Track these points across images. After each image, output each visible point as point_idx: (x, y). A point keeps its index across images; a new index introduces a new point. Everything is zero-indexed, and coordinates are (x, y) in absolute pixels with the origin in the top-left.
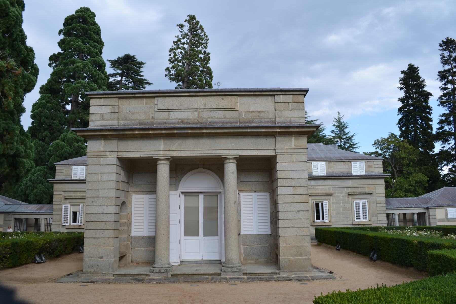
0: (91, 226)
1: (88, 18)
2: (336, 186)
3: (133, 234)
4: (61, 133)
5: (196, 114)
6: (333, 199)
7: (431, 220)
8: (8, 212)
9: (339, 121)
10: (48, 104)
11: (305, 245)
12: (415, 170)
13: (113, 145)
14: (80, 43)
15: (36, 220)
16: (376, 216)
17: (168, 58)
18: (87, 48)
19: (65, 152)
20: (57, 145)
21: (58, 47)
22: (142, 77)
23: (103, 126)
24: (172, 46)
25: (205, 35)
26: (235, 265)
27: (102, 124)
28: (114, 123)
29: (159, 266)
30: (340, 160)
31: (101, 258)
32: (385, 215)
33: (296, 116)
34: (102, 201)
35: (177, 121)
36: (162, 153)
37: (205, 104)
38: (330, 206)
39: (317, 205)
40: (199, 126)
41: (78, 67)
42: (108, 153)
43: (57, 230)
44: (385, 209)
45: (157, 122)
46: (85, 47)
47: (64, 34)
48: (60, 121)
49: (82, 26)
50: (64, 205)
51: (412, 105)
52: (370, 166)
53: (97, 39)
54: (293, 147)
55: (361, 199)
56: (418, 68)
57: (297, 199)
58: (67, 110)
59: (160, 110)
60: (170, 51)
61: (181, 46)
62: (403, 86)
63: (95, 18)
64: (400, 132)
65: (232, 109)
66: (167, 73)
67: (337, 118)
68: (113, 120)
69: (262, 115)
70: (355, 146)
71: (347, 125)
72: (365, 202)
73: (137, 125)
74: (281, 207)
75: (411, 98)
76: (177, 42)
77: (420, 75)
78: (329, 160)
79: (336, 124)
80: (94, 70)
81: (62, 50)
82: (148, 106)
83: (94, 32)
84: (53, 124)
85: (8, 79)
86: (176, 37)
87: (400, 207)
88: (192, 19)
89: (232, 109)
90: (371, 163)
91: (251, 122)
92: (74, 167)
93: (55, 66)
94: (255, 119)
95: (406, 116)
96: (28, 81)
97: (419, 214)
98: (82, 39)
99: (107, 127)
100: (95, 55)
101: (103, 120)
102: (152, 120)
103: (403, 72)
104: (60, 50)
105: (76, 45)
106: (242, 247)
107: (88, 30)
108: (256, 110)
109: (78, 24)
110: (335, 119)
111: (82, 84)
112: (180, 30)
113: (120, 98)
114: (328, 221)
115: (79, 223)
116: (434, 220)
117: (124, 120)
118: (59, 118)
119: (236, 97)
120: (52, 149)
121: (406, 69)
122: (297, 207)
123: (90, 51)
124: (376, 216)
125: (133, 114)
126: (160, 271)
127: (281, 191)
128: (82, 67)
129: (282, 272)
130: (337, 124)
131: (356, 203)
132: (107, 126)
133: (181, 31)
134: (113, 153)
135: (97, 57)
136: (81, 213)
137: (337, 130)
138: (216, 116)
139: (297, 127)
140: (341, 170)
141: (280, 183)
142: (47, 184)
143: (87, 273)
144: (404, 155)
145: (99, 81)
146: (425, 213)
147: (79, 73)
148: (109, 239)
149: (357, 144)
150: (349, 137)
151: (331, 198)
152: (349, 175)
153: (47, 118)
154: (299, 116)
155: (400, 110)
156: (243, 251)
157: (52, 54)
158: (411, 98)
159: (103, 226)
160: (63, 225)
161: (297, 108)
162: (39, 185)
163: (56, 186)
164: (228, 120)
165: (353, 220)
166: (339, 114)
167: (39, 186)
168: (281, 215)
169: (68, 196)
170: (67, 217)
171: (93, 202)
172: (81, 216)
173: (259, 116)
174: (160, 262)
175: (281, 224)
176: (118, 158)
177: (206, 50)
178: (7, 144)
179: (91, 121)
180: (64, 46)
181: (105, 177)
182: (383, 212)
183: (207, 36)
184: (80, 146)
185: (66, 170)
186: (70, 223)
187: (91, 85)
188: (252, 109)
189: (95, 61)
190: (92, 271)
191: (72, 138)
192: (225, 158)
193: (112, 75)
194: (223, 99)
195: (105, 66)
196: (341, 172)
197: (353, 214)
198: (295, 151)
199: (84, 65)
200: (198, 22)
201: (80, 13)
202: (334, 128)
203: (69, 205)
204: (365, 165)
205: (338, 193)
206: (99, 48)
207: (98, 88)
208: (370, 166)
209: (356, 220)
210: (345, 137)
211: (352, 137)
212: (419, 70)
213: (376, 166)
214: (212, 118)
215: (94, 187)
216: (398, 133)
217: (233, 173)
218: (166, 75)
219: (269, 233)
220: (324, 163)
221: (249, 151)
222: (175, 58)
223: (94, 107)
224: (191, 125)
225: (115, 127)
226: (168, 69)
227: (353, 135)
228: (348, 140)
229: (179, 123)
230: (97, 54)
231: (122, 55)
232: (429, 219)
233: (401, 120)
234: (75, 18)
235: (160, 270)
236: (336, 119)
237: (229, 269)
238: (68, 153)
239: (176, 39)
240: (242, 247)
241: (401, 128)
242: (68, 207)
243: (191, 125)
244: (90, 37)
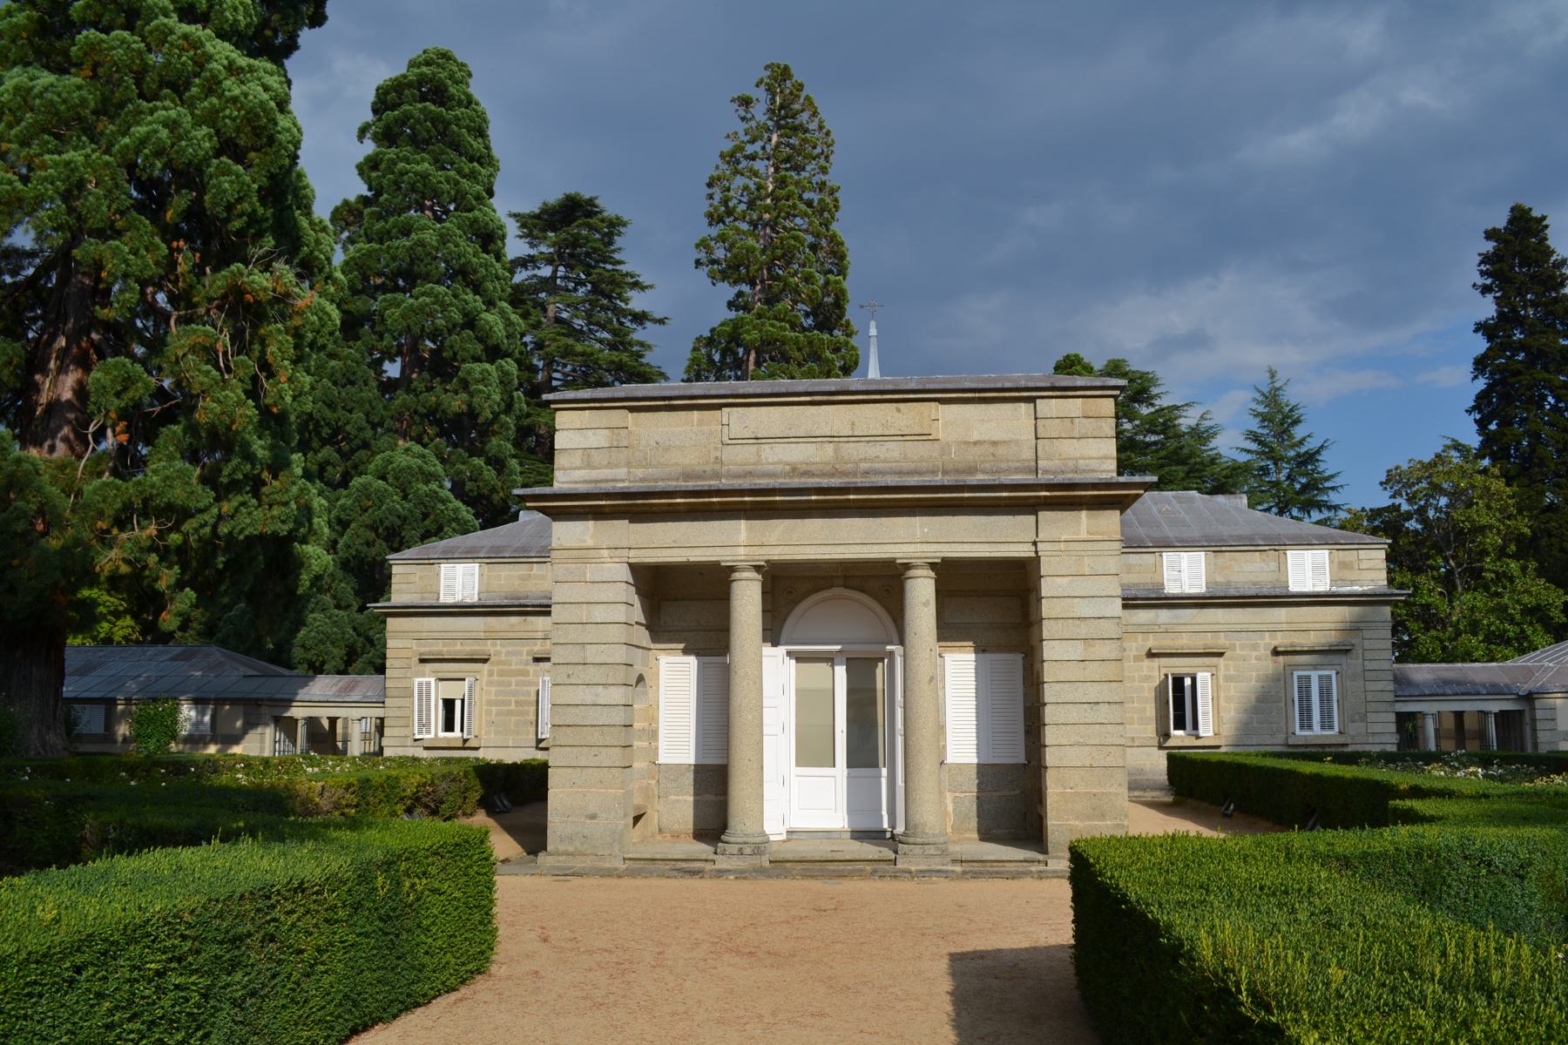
0: (565, 736)
1: (449, 82)
2: (1238, 627)
3: (661, 760)
4: (374, 454)
5: (830, 448)
6: (1227, 667)
7: (1540, 734)
8: (257, 700)
9: (1272, 398)
10: (333, 363)
11: (1112, 790)
12: (1524, 569)
13: (620, 530)
14: (426, 165)
15: (333, 721)
16: (1364, 718)
17: (705, 207)
18: (448, 182)
19: (391, 511)
20: (365, 487)
21: (359, 178)
22: (618, 267)
23: (591, 482)
24: (717, 167)
25: (821, 128)
26: (931, 840)
27: (587, 478)
28: (621, 477)
29: (739, 840)
30: (1250, 544)
31: (593, 817)
32: (1392, 718)
33: (1093, 453)
34: (592, 674)
35: (779, 468)
36: (742, 551)
37: (853, 424)
38: (1217, 687)
39: (1178, 681)
40: (835, 482)
41: (422, 243)
42: (605, 553)
43: (401, 752)
44: (1391, 697)
45: (729, 471)
46: (442, 179)
47: (375, 138)
48: (367, 415)
49: (431, 112)
50: (417, 680)
51: (1522, 346)
52: (1344, 565)
53: (479, 150)
54: (1084, 536)
55: (1315, 667)
56: (1544, 218)
57: (1094, 671)
58: (389, 378)
59: (735, 441)
60: (710, 185)
61: (744, 163)
62: (1493, 282)
63: (470, 81)
64: (1481, 438)
65: (924, 437)
66: (702, 256)
67: (1266, 391)
68: (617, 466)
69: (1001, 451)
70: (1327, 484)
71: (1300, 411)
72: (1329, 677)
73: (677, 480)
74: (1050, 693)
75: (1519, 322)
76: (732, 155)
77: (1551, 243)
78: (1215, 544)
79: (1261, 409)
80: (470, 250)
81: (370, 189)
82: (705, 428)
83: (469, 129)
84: (348, 423)
85: (276, 322)
86: (728, 136)
87: (1441, 691)
89: (924, 437)
90: (1350, 556)
91: (972, 470)
92: (445, 568)
93: (351, 241)
94: (982, 462)
95: (1503, 382)
96: (320, 319)
97: (1502, 716)
98: (434, 151)
99: (603, 485)
100: (474, 202)
101: (589, 465)
102: (717, 467)
103: (1490, 235)
104: (364, 190)
105: (416, 174)
106: (949, 797)
107: (449, 123)
108: (987, 438)
109: (420, 106)
110: (1259, 391)
111: (436, 297)
112: (743, 114)
113: (632, 409)
114: (1211, 734)
115: (462, 730)
116: (1549, 734)
117: (644, 467)
118: (367, 406)
119: (933, 404)
120: (350, 502)
121: (1500, 221)
122: (1093, 693)
123: (458, 192)
124: (1364, 718)
125: (667, 449)
126: (741, 852)
127: (1050, 651)
128: (435, 243)
129: (1053, 858)
130: (1266, 410)
131: (1299, 677)
132: (601, 481)
133: (743, 119)
134: (618, 552)
135: (480, 210)
136: (470, 704)
137: (1266, 431)
138: (882, 457)
139: (1095, 486)
140: (1253, 578)
141: (1048, 629)
142: (336, 611)
143: (558, 854)
144: (1484, 521)
145: (489, 285)
146: (1521, 712)
147: (426, 261)
148: (613, 770)
149: (1332, 476)
150: (1307, 452)
151: (1221, 661)
152: (1278, 592)
153: (329, 406)
154: (1102, 453)
155: (1480, 364)
156: (950, 808)
157: (339, 203)
158: (1519, 322)
159: (595, 737)
160: (417, 737)
161: (1095, 434)
162: (314, 615)
163: (393, 624)
164: (912, 466)
165: (1290, 731)
166: (1273, 376)
167: (315, 619)
168: (1050, 714)
169: (430, 653)
170: (428, 716)
171: (569, 676)
172: (470, 713)
173: (993, 455)
174: (740, 825)
175: (1051, 736)
176: (629, 564)
177: (824, 178)
178: (271, 506)
179: (559, 469)
180: (378, 177)
181: (599, 614)
182: (1383, 707)
183: (828, 134)
184: (436, 492)
185: (421, 577)
186: (436, 732)
187: (465, 301)
188: (975, 437)
189: (476, 220)
190: (571, 849)
191: (409, 468)
192: (907, 567)
193: (524, 262)
194: (899, 410)
195: (503, 237)
196: (1254, 584)
197: (1290, 713)
198: (1089, 546)
199: (442, 235)
201: (424, 69)
202: (1254, 424)
203: (432, 680)
204: (1331, 562)
205: (1242, 648)
206: (486, 180)
207: (484, 307)
208: (1344, 565)
209: (1298, 732)
211: (1318, 452)
212: (1546, 227)
213: (1364, 565)
214: (871, 461)
215: (572, 638)
216: (1473, 440)
217: (926, 604)
218: (698, 263)
219: (1022, 760)
221: (967, 547)
222: (727, 206)
223: (565, 433)
224: (818, 480)
225: (620, 485)
226: (703, 244)
227: (1322, 447)
229: (787, 475)
230: (478, 198)
231: (554, 196)
232: (1534, 730)
233: (1482, 398)
234: (410, 85)
235: (740, 849)
236: (1263, 394)
237: (917, 849)
238: (399, 517)
239: (728, 146)
240: (949, 797)
241: (1482, 424)
242: (428, 684)
243: (818, 480)
244: (457, 146)
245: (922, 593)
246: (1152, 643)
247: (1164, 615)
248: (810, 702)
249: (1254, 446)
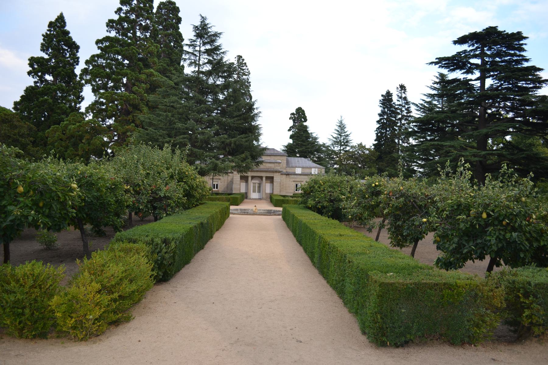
25: (248, 69)
79: (338, 124)
88: (240, 57)
103: (382, 96)
121: (384, 93)
155: (378, 122)
200: (243, 60)
202: (337, 128)
210: (343, 134)
220: (301, 169)
228: (347, 136)
245: (264, 179)
246: (294, 180)
247: (295, 176)
248: (254, 187)
249: (337, 132)
